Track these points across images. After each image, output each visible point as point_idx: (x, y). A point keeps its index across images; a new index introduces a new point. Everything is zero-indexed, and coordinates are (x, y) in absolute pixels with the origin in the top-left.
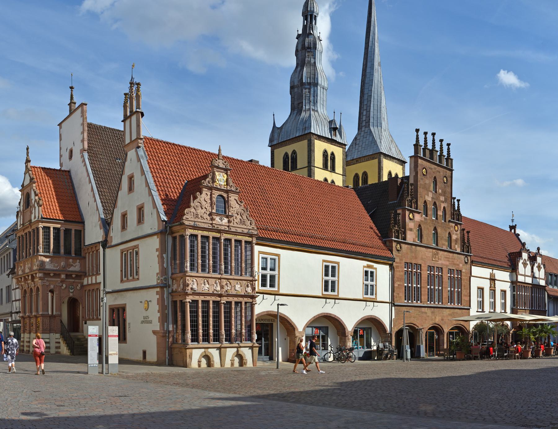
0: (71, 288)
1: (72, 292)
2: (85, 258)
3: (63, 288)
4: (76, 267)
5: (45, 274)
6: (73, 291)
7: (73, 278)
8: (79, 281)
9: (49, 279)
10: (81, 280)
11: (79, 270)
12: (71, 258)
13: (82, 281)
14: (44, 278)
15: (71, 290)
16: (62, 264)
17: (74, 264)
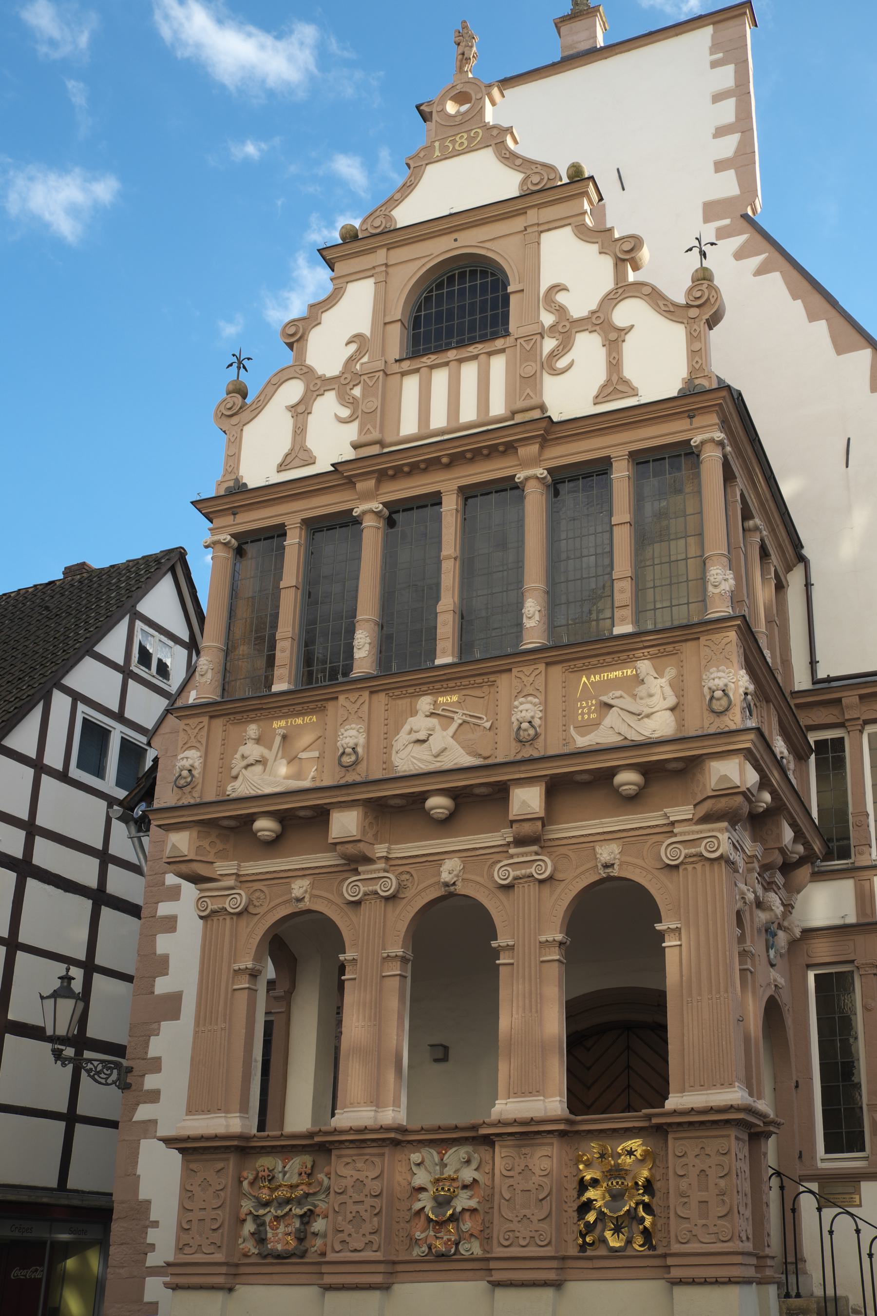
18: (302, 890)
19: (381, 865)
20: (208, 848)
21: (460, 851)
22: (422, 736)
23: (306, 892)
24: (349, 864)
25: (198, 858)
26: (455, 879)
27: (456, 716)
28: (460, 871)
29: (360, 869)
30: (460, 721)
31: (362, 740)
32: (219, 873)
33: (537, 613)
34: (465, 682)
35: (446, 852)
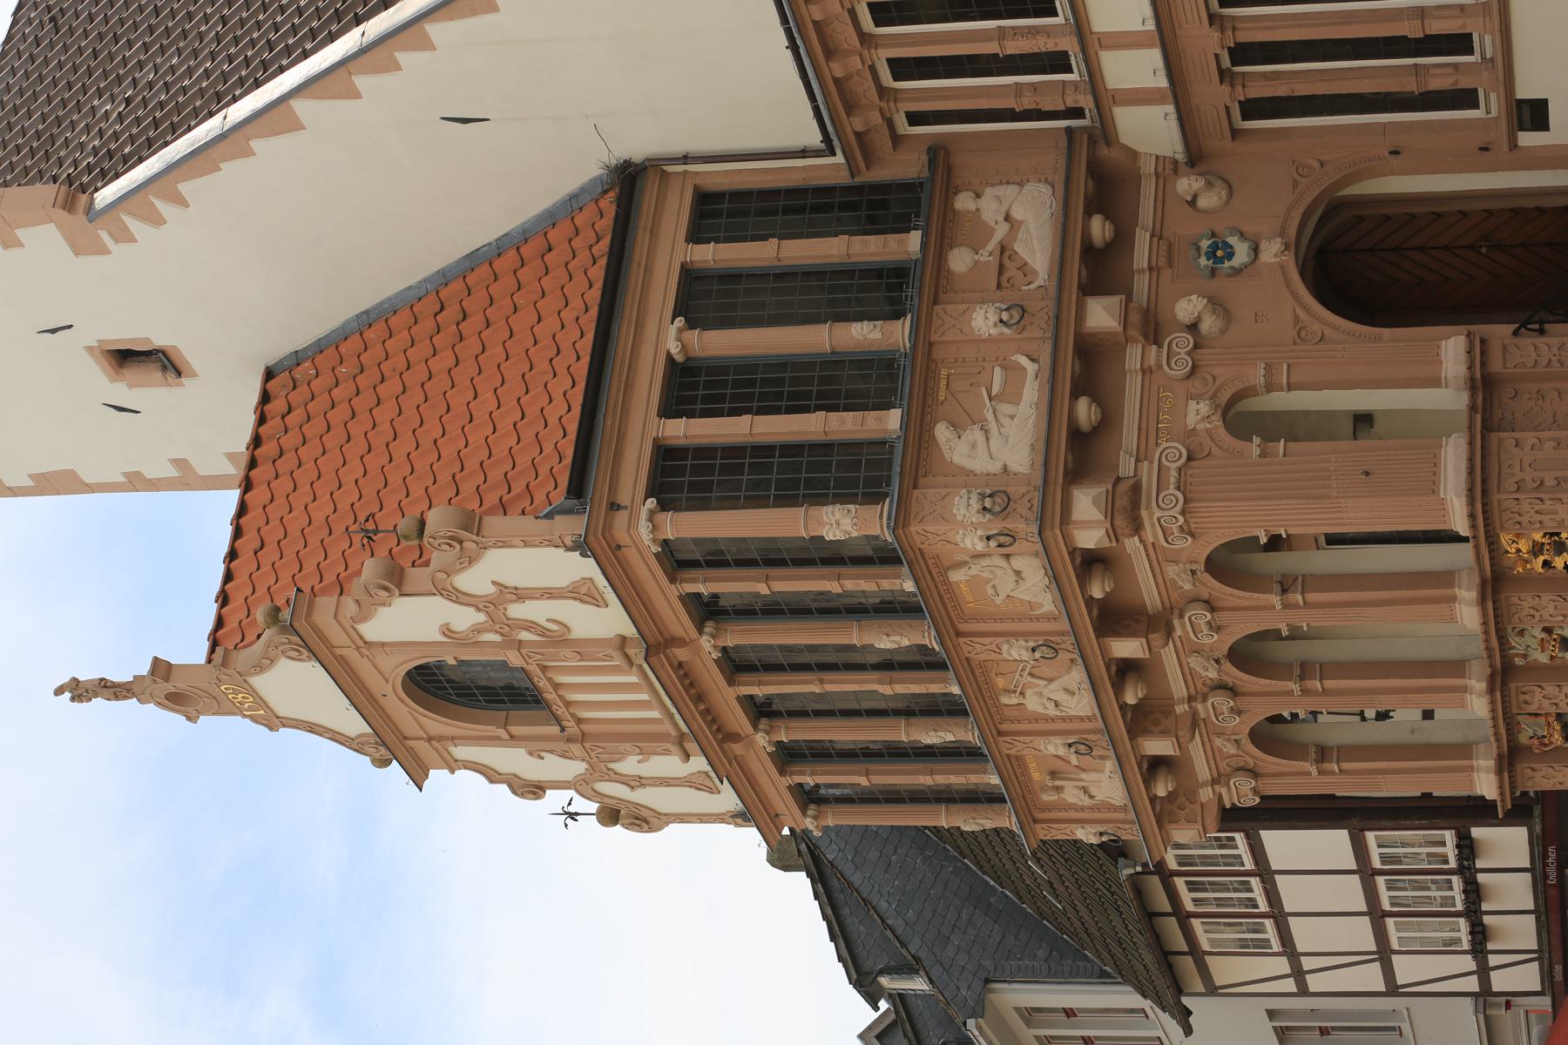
0: (1212, 254)
1: (1256, 250)
2: (937, 153)
3: (1208, 325)
4: (1017, 214)
5: (1078, 473)
6: (1242, 236)
7: (1122, 240)
8: (1148, 191)
9: (1129, 435)
10: (1135, 179)
11: (1045, 190)
12: (941, 259)
13: (1148, 167)
14: (1118, 479)
15: (1230, 255)
16: (984, 321)
17: (991, 231)
18: (1229, 745)
19: (1200, 707)
20: (1187, 811)
21: (1178, 658)
22: (1051, 706)
23: (1228, 740)
24: (1199, 725)
25: (1199, 819)
26: (1213, 662)
27: (1023, 680)
28: (1202, 656)
29: (1203, 716)
30: (1029, 678)
31: (1059, 741)
32: (1211, 796)
33: (891, 638)
34: (981, 679)
35: (1181, 665)
